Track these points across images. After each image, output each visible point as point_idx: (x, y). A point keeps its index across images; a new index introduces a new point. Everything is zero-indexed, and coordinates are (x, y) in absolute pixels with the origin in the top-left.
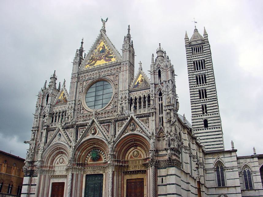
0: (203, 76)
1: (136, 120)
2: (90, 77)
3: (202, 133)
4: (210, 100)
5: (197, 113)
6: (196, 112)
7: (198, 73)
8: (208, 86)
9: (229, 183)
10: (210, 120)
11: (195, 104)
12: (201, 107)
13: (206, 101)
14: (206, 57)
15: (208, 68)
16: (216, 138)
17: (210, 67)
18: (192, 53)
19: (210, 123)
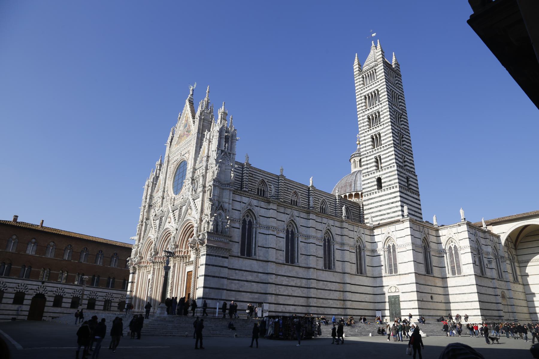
0: (377, 114)
1: (192, 203)
2: (176, 158)
3: (375, 198)
4: (385, 148)
5: (369, 170)
6: (367, 168)
7: (370, 111)
8: (382, 127)
9: (401, 269)
10: (385, 178)
11: (366, 157)
12: (374, 160)
13: (380, 150)
14: (379, 84)
15: (383, 100)
16: (392, 203)
17: (385, 99)
18: (363, 84)
19: (385, 182)
